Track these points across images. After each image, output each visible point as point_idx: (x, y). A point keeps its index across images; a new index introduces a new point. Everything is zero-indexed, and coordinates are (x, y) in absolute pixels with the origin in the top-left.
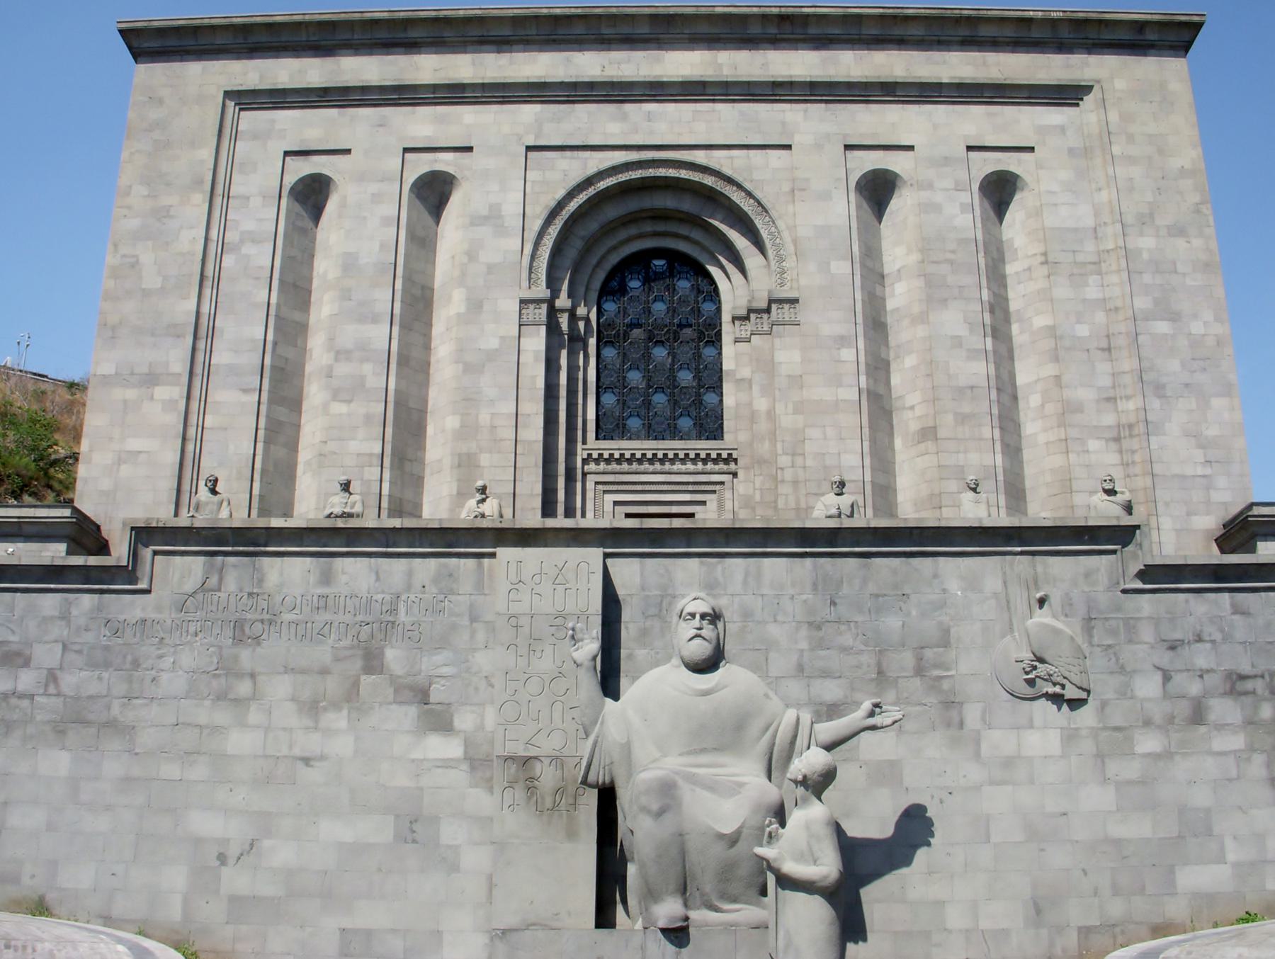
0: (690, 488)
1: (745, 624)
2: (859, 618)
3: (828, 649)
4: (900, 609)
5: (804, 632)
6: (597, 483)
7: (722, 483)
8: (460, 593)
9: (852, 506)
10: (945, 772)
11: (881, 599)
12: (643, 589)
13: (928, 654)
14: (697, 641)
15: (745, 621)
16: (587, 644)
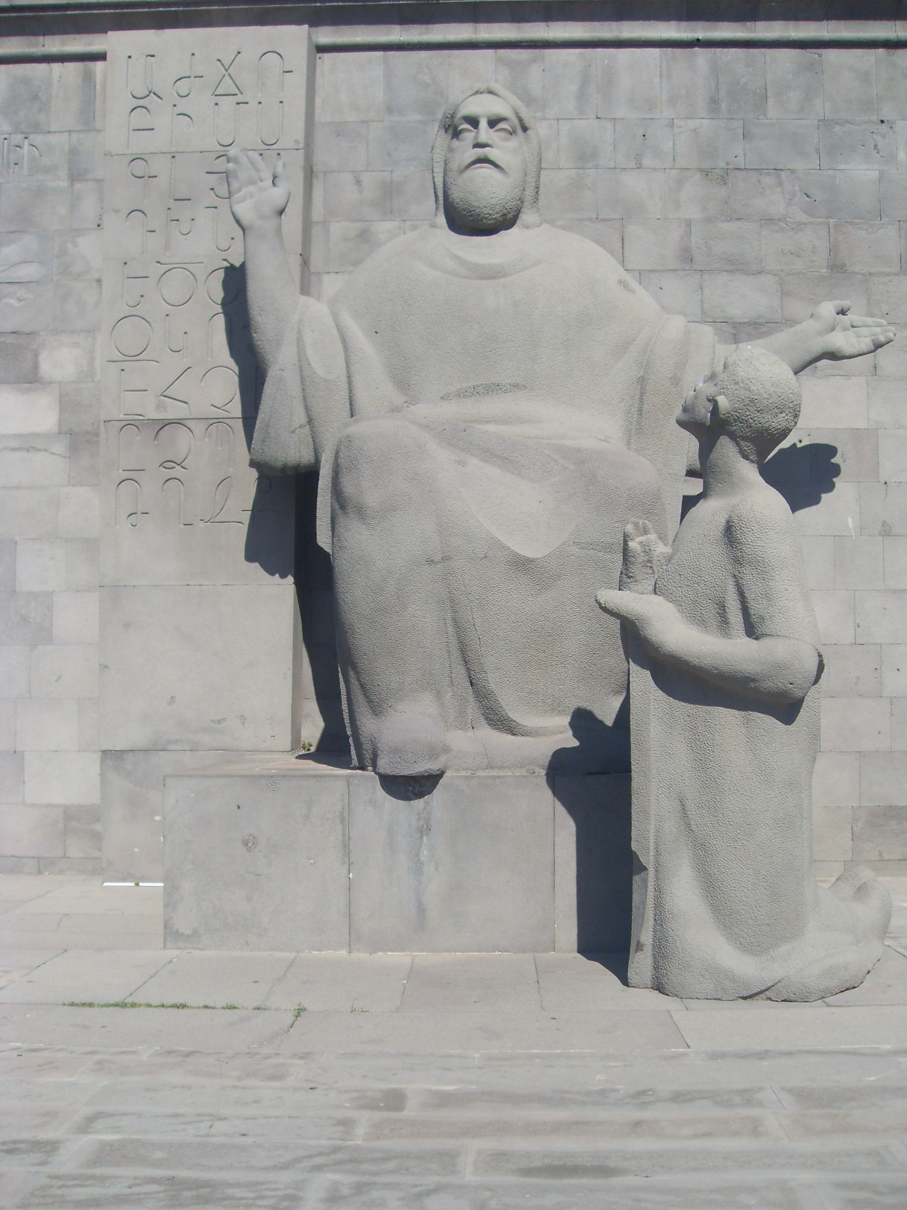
1: (581, 171)
2: (799, 165)
4: (876, 146)
8: (52, 129)
11: (837, 129)
12: (390, 111)
14: (485, 170)
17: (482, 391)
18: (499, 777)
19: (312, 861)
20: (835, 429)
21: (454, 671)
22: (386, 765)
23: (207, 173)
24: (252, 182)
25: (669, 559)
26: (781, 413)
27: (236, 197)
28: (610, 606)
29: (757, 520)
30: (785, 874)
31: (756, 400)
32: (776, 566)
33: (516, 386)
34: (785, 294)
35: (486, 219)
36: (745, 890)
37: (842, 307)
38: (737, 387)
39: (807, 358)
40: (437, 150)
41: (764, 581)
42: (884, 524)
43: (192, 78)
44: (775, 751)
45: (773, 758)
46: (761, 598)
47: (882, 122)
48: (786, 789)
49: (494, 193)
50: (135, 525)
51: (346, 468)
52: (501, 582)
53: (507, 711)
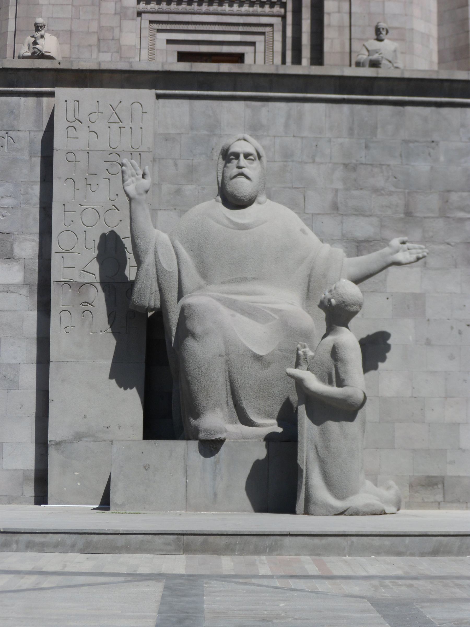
0: (241, 29)
1: (285, 163)
2: (392, 162)
3: (361, 189)
4: (429, 154)
5: (339, 173)
6: (151, 22)
7: (271, 25)
8: (20, 129)
9: (395, 51)
10: (465, 306)
11: (411, 145)
12: (192, 129)
13: (454, 197)
15: (286, 161)
16: (137, 179)
17: (239, 281)
18: (247, 442)
19: (172, 475)
21: (229, 400)
22: (202, 436)
23: (105, 161)
24: (133, 176)
25: (313, 358)
26: (354, 306)
27: (126, 183)
28: (291, 374)
33: (254, 278)
34: (382, 226)
36: (337, 476)
38: (338, 296)
39: (384, 265)
40: (220, 165)
42: (427, 339)
43: (97, 114)
47: (433, 142)
49: (246, 190)
50: (68, 332)
51: (188, 317)
53: (250, 417)
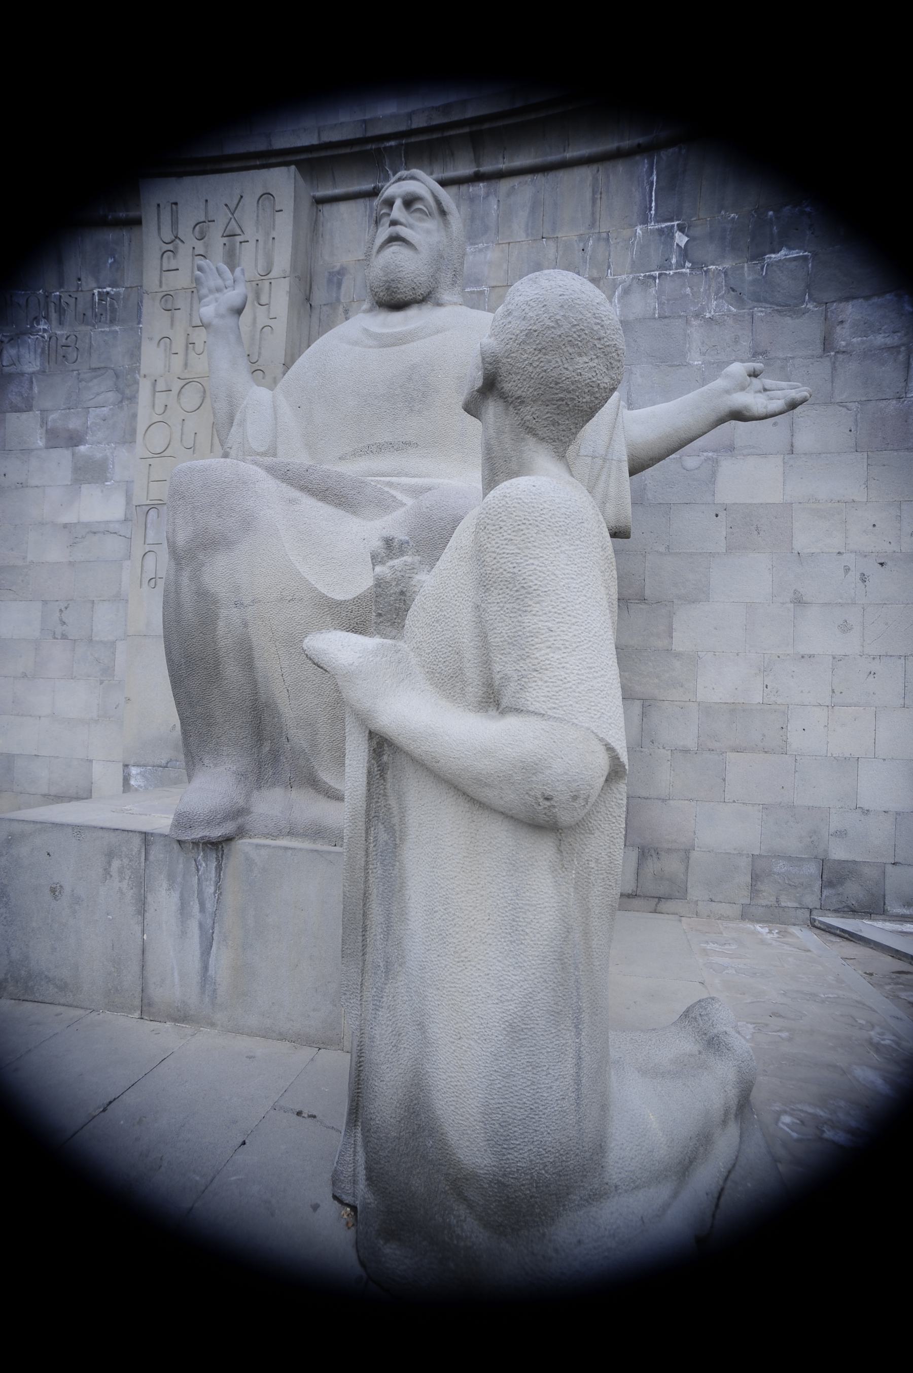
14: (395, 248)
19: (110, 917)
20: (751, 504)
24: (218, 290)
26: (580, 355)
29: (509, 509)
30: (536, 1105)
31: (535, 331)
32: (535, 587)
35: (395, 293)
37: (754, 369)
38: (509, 319)
41: (515, 615)
42: (795, 592)
44: (529, 905)
45: (524, 916)
46: (509, 643)
48: (544, 968)
52: (309, 627)
